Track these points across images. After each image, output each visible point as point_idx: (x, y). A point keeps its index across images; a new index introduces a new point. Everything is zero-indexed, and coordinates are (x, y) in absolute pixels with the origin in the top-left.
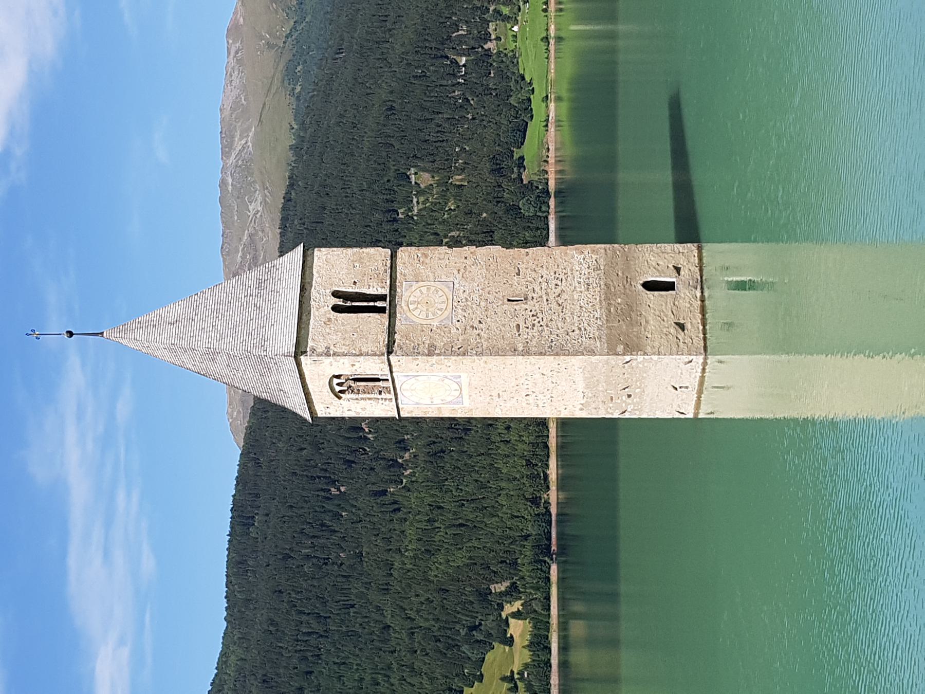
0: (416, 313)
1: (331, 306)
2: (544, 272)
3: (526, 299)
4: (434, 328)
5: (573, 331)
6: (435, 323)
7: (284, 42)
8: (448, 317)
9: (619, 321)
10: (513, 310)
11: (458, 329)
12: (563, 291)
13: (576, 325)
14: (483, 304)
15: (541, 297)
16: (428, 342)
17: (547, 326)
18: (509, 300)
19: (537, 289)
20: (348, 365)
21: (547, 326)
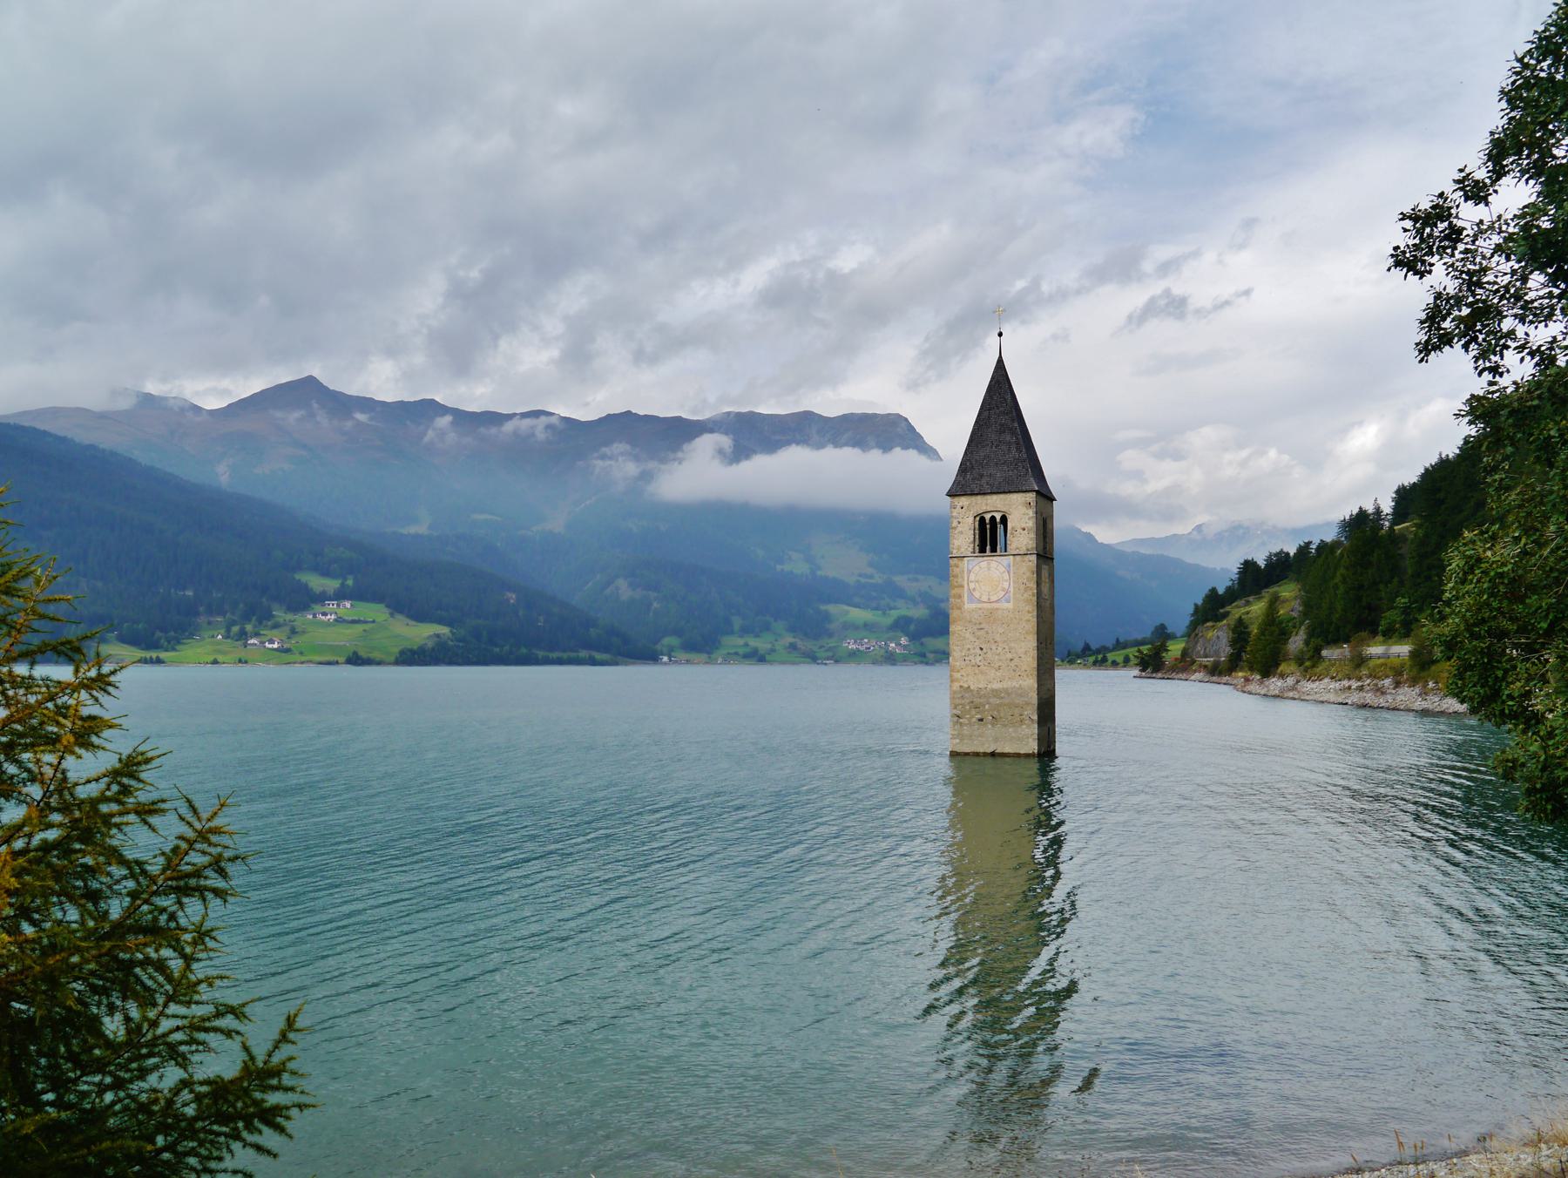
20: (1024, 525)
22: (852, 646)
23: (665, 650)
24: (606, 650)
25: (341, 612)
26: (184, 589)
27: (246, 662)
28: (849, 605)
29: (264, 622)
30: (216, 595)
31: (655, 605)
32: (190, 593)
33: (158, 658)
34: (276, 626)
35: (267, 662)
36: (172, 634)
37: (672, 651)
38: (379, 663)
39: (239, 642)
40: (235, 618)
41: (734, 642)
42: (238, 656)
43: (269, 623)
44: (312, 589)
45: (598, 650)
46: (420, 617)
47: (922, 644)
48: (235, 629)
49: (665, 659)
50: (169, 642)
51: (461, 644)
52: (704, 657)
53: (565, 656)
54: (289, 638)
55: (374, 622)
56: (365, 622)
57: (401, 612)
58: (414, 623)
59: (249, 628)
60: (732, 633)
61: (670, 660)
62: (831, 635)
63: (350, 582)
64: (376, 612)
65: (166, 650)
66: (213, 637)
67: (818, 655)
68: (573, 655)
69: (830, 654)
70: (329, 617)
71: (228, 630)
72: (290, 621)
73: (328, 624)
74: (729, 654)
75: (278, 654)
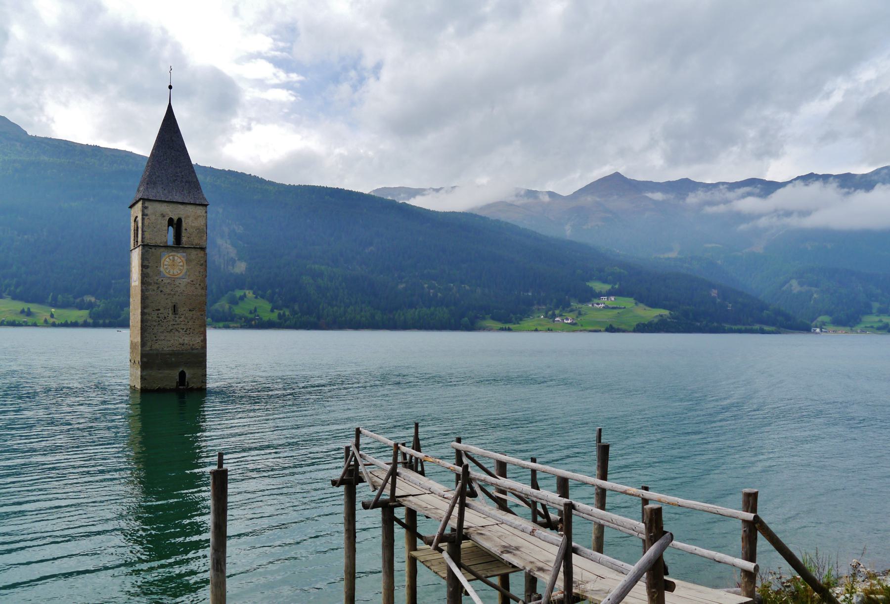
0: (168, 260)
1: (172, 217)
2: (190, 323)
3: (175, 314)
4: (158, 268)
5: (156, 337)
6: (162, 269)
8: (164, 275)
9: (161, 359)
10: (168, 307)
11: (157, 280)
12: (179, 332)
13: (159, 338)
14: (172, 293)
15: (176, 321)
16: (150, 265)
17: (159, 324)
18: (175, 305)
19: (181, 319)
21: (159, 324)
23: (818, 324)
24: (773, 324)
25: (608, 303)
26: (528, 291)
27: (552, 330)
29: (566, 309)
30: (543, 294)
31: (815, 296)
32: (530, 294)
33: (509, 327)
34: (572, 311)
35: (563, 331)
36: (518, 315)
37: (825, 325)
38: (624, 331)
39: (551, 320)
40: (552, 307)
41: (872, 319)
42: (547, 327)
43: (569, 309)
44: (595, 291)
45: (767, 324)
46: (653, 305)
48: (550, 313)
49: (818, 330)
50: (516, 319)
51: (675, 321)
52: (849, 328)
53: (743, 328)
54: (577, 317)
55: (625, 308)
56: (620, 308)
57: (642, 302)
59: (557, 312)
60: (871, 313)
61: (821, 331)
63: (617, 286)
64: (627, 303)
65: (515, 324)
66: (539, 317)
68: (748, 327)
71: (547, 313)
72: (579, 308)
73: (600, 310)
74: (866, 327)
75: (570, 326)
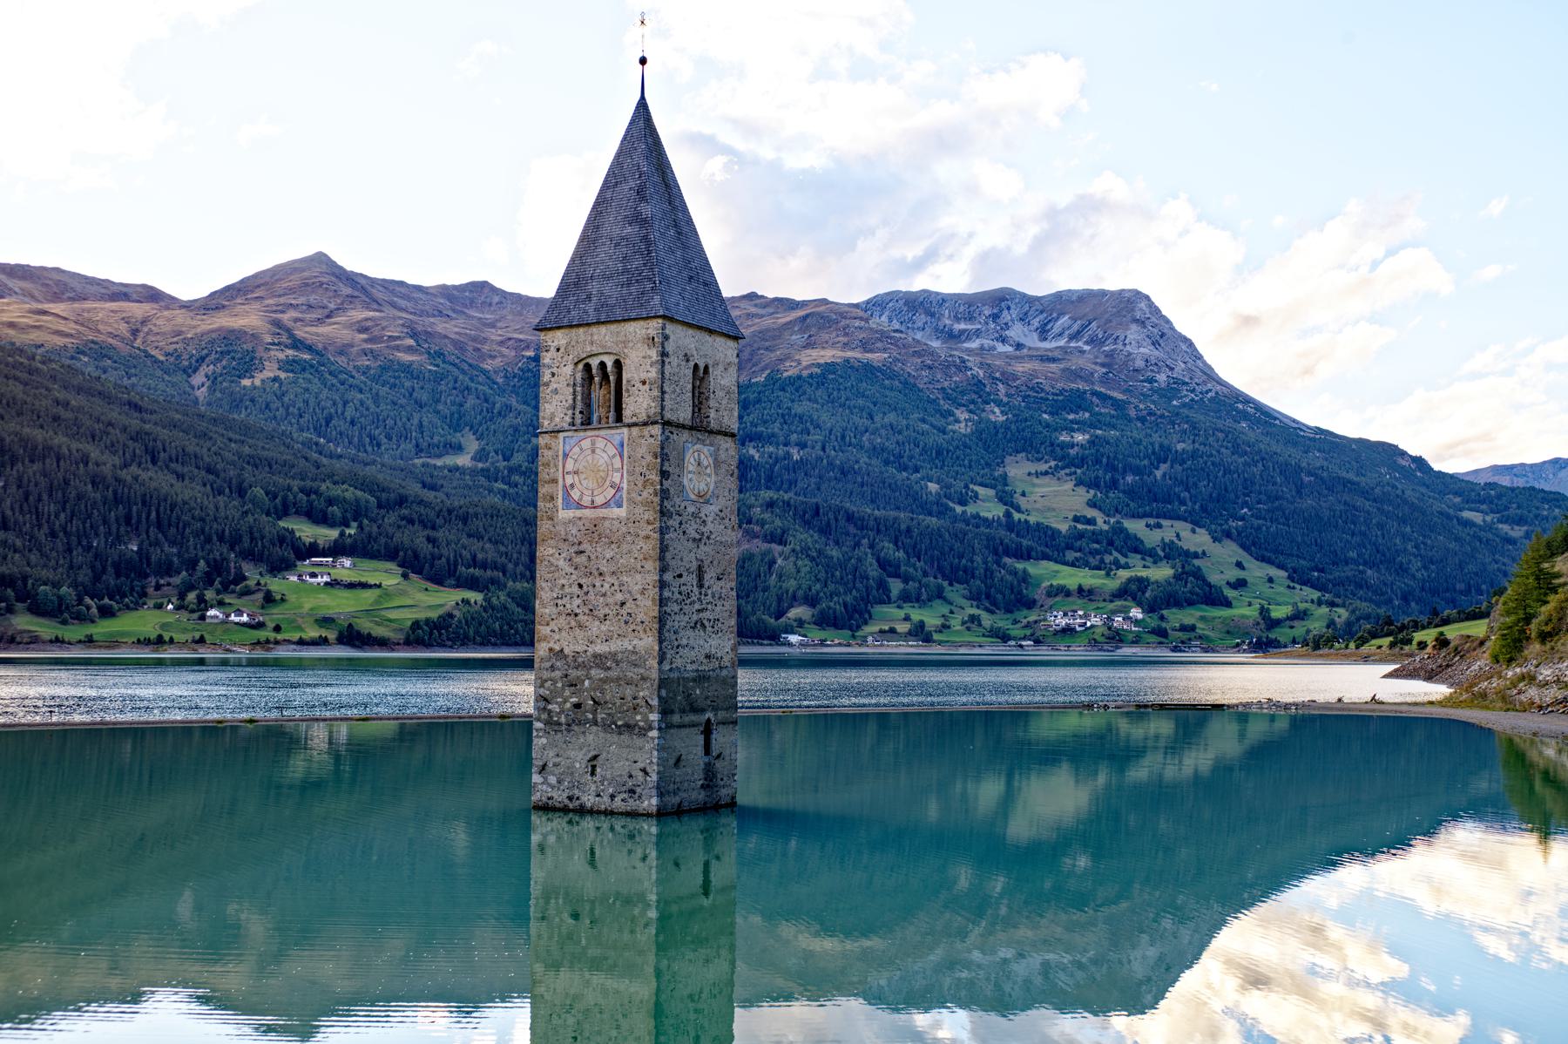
7: (139, 349)
22: (1063, 622)
28: (1056, 562)
34: (247, 592)
36: (106, 601)
39: (196, 615)
47: (1162, 618)
57: (419, 572)
58: (436, 587)
59: (210, 595)
60: (889, 603)
62: (1030, 604)
64: (386, 575)
67: (1013, 633)
69: (1028, 632)
70: (319, 579)
71: (182, 596)
74: (881, 631)
